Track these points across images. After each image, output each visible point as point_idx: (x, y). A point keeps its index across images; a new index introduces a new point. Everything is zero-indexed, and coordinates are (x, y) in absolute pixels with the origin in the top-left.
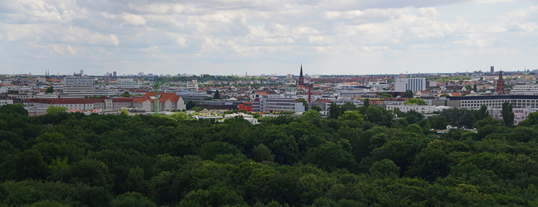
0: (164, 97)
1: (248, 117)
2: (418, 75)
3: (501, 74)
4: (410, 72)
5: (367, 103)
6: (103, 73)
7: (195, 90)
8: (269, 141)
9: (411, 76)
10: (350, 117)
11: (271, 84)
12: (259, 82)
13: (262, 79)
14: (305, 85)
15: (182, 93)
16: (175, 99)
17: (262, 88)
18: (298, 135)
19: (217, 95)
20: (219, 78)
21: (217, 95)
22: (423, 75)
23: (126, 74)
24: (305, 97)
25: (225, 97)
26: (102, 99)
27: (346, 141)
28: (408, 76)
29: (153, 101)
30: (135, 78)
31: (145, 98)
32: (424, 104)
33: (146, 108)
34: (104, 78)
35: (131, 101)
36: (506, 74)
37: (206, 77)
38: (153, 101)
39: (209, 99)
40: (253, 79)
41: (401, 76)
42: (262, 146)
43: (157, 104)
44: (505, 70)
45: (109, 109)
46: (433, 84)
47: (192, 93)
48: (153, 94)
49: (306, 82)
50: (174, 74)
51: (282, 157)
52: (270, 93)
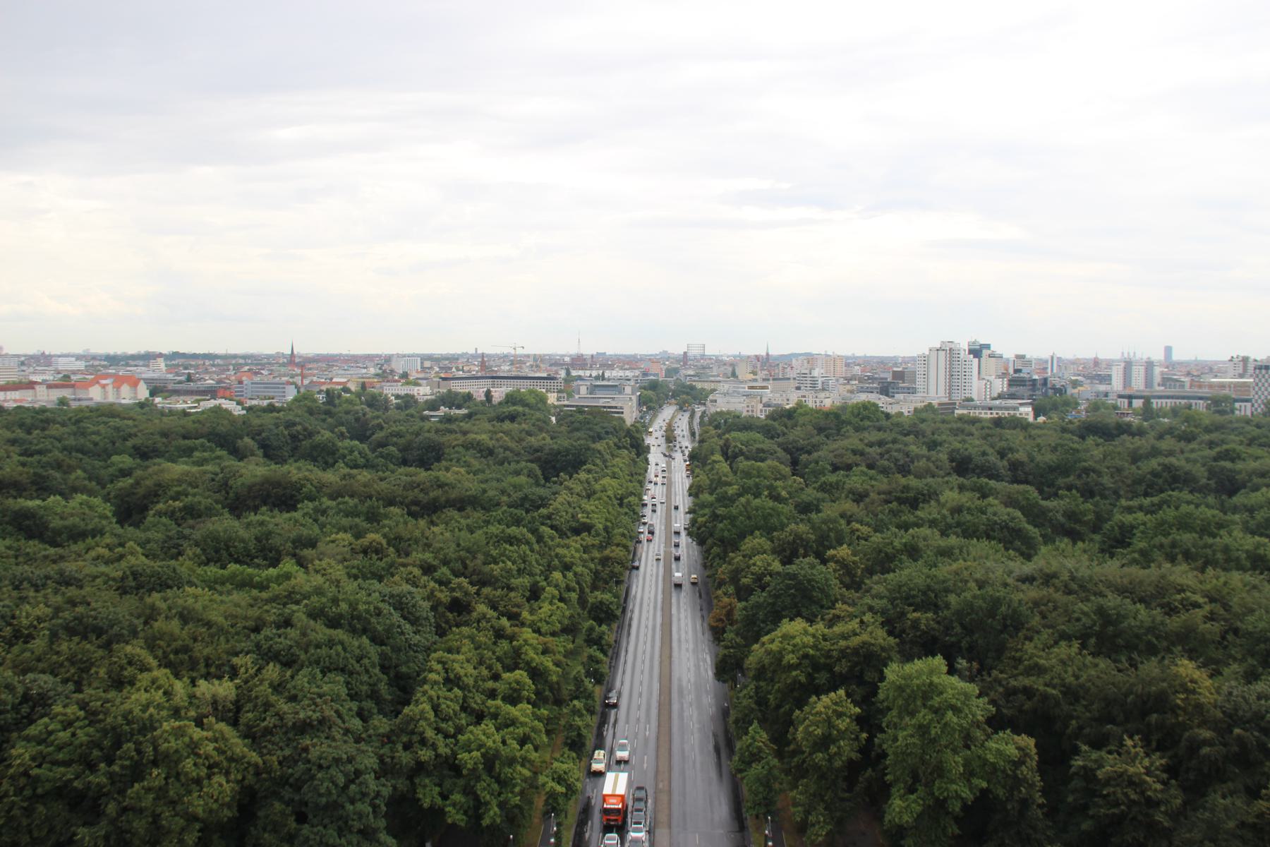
0: (119, 381)
1: (227, 405)
2: (412, 356)
3: (483, 355)
4: (406, 352)
5: (364, 386)
6: (32, 350)
7: (160, 370)
8: (255, 435)
9: (744, 373)
10: (349, 401)
11: (256, 363)
12: (241, 361)
13: (245, 357)
14: (297, 365)
15: (144, 376)
16: (134, 383)
17: (246, 368)
18: (290, 425)
19: (189, 379)
20: (195, 356)
21: (189, 379)
22: (418, 355)
23: (65, 352)
24: (298, 380)
25: (200, 380)
26: (31, 385)
27: (343, 429)
28: (404, 356)
29: (104, 386)
30: (79, 357)
31: (95, 382)
32: (419, 385)
33: (96, 395)
34: (32, 357)
35: (73, 386)
36: (488, 356)
37: (176, 355)
38: (104, 386)
39: (180, 382)
40: (235, 356)
41: (398, 355)
42: (247, 440)
43: (110, 388)
44: (487, 352)
45: (44, 398)
46: (427, 364)
47: (155, 375)
48: (106, 376)
49: (297, 360)
50: (132, 350)
51: (269, 452)
52: (256, 373)
